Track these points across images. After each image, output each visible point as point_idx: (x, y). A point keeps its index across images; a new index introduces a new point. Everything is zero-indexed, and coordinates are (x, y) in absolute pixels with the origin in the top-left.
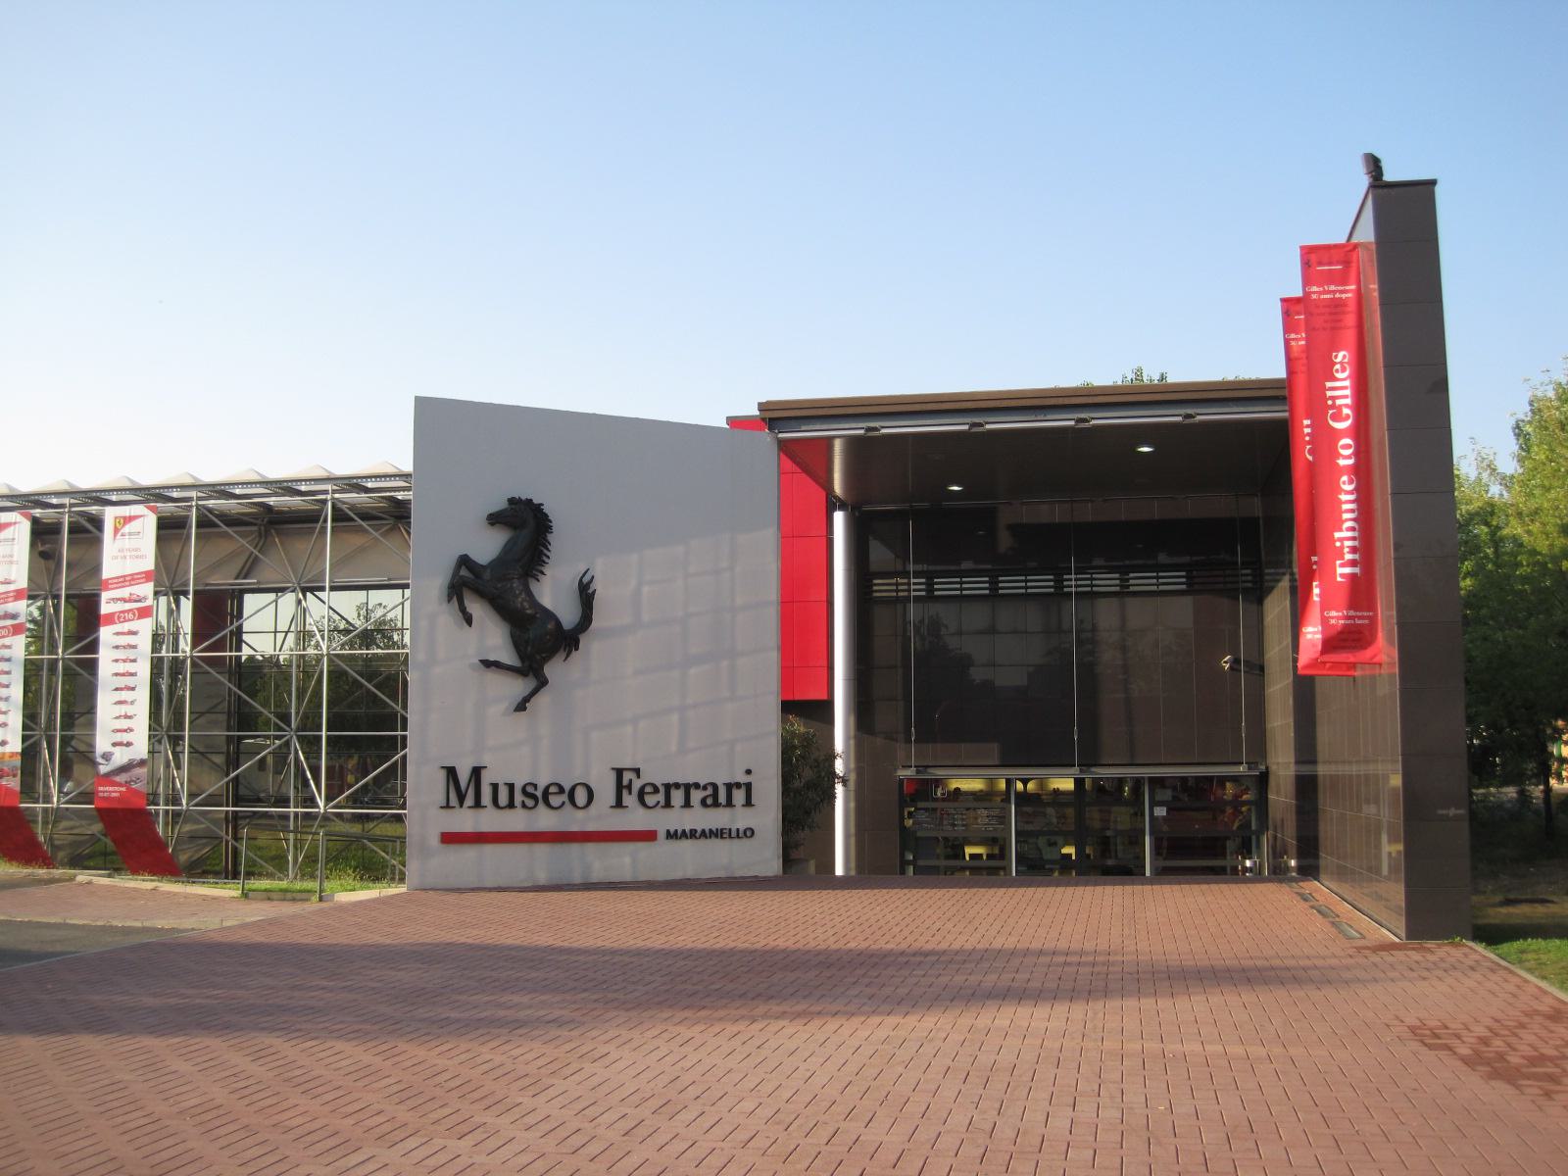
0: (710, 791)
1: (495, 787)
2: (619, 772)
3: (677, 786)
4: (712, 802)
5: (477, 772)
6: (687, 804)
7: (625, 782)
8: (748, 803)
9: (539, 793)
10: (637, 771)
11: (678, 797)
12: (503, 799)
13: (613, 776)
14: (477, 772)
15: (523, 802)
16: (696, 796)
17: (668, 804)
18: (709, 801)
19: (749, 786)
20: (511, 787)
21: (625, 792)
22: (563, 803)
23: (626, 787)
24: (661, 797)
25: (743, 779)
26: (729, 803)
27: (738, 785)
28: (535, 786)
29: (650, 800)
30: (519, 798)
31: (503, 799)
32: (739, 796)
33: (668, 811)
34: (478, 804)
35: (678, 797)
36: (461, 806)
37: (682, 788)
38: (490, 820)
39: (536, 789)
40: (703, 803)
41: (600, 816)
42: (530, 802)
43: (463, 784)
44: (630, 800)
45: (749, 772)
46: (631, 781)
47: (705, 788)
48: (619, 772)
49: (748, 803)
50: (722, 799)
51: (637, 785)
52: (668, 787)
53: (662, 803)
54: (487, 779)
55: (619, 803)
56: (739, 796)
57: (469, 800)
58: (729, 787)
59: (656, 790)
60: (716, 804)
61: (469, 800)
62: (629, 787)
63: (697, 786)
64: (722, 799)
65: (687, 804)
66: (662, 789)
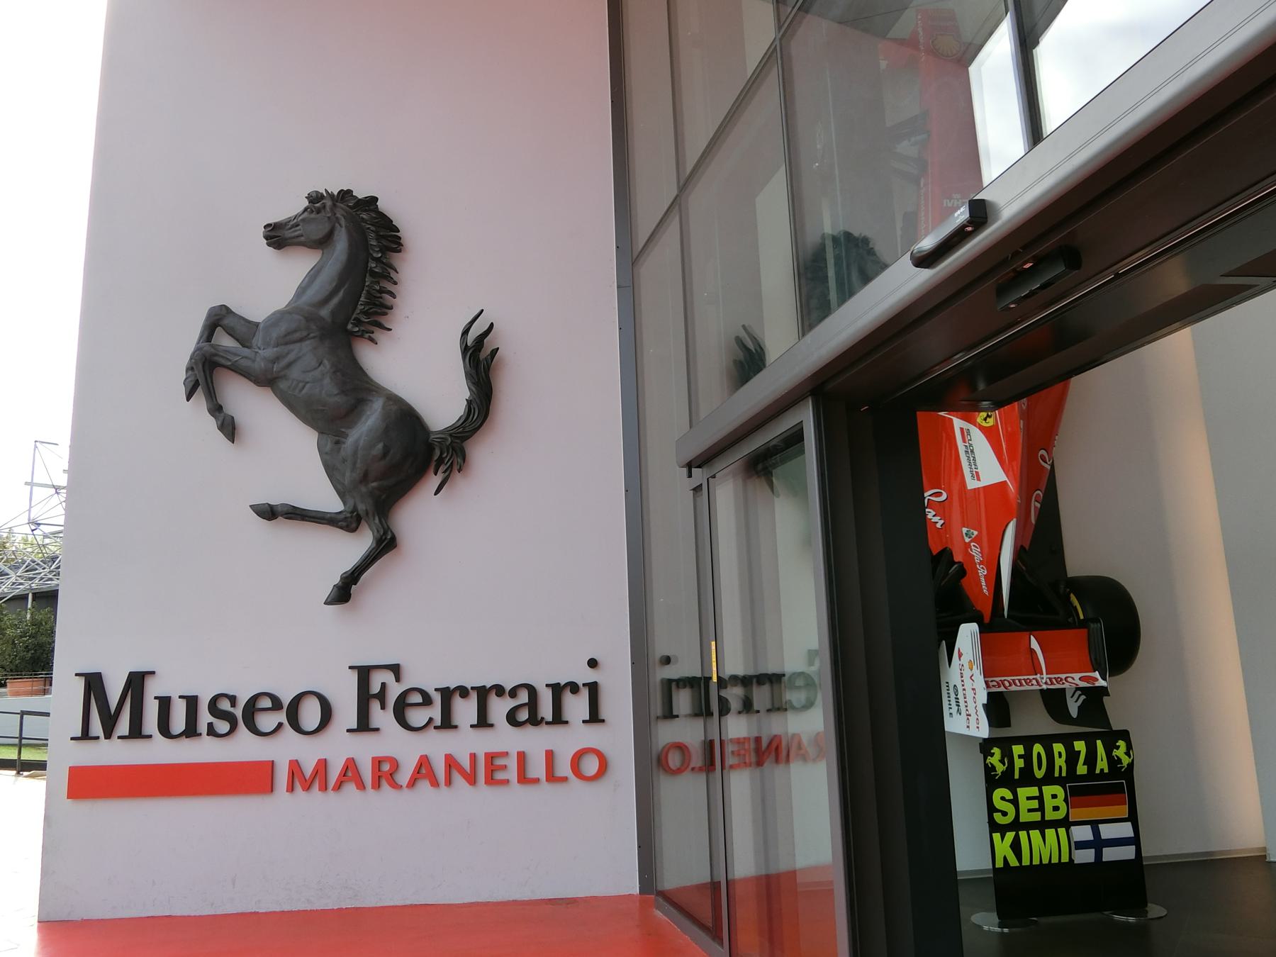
0: (523, 697)
1: (165, 703)
2: (364, 673)
3: (463, 692)
4: (528, 714)
5: (136, 682)
6: (483, 722)
7: (375, 688)
8: (594, 717)
9: (238, 712)
10: (396, 669)
11: (465, 711)
12: (178, 721)
13: (354, 677)
14: (136, 682)
15: (210, 725)
16: (499, 708)
17: (447, 723)
18: (523, 715)
19: (593, 688)
20: (192, 702)
21: (375, 706)
22: (280, 725)
23: (375, 696)
24: (435, 712)
25: (584, 675)
26: (558, 719)
27: (574, 688)
28: (233, 700)
29: (417, 717)
30: (205, 717)
31: (178, 721)
32: (577, 707)
33: (447, 735)
34: (136, 732)
35: (465, 711)
36: (108, 735)
37: (474, 697)
38: (158, 751)
39: (233, 704)
40: (512, 718)
41: (339, 746)
42: (223, 727)
43: (114, 700)
44: (382, 717)
45: (593, 663)
46: (383, 685)
47: (513, 693)
48: (364, 673)
49: (594, 717)
50: (546, 710)
51: (394, 691)
52: (447, 694)
53: (438, 722)
54: (153, 689)
55: (364, 725)
56: (577, 707)
57: (123, 726)
58: (557, 690)
59: (427, 701)
60: (535, 720)
61: (123, 726)
62: (382, 696)
63: (499, 690)
64: (546, 710)
65: (483, 722)
66: (437, 698)
